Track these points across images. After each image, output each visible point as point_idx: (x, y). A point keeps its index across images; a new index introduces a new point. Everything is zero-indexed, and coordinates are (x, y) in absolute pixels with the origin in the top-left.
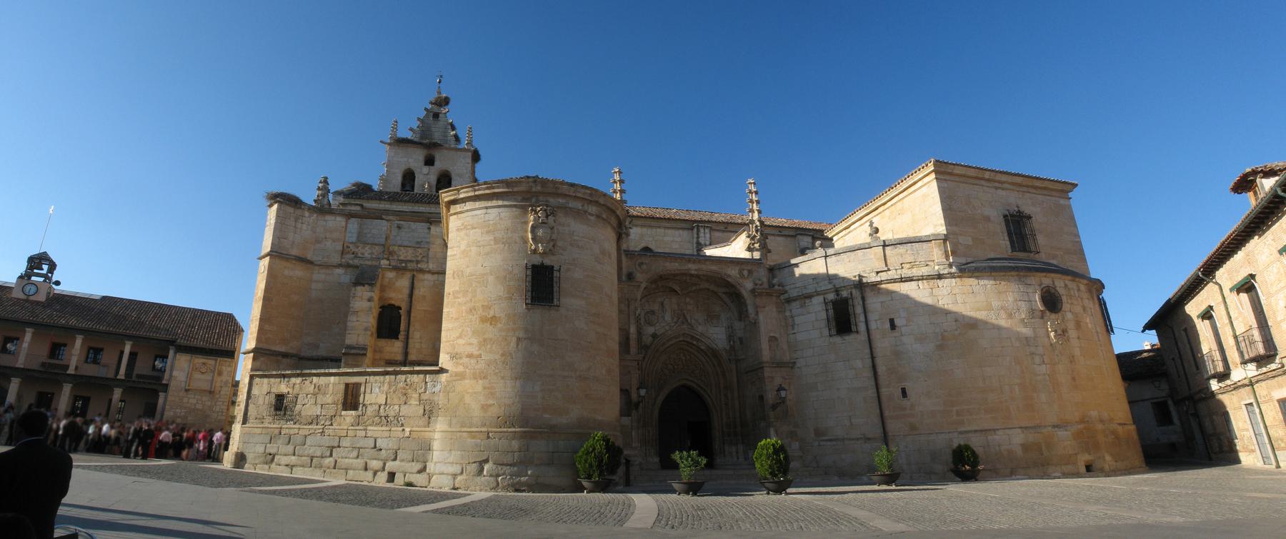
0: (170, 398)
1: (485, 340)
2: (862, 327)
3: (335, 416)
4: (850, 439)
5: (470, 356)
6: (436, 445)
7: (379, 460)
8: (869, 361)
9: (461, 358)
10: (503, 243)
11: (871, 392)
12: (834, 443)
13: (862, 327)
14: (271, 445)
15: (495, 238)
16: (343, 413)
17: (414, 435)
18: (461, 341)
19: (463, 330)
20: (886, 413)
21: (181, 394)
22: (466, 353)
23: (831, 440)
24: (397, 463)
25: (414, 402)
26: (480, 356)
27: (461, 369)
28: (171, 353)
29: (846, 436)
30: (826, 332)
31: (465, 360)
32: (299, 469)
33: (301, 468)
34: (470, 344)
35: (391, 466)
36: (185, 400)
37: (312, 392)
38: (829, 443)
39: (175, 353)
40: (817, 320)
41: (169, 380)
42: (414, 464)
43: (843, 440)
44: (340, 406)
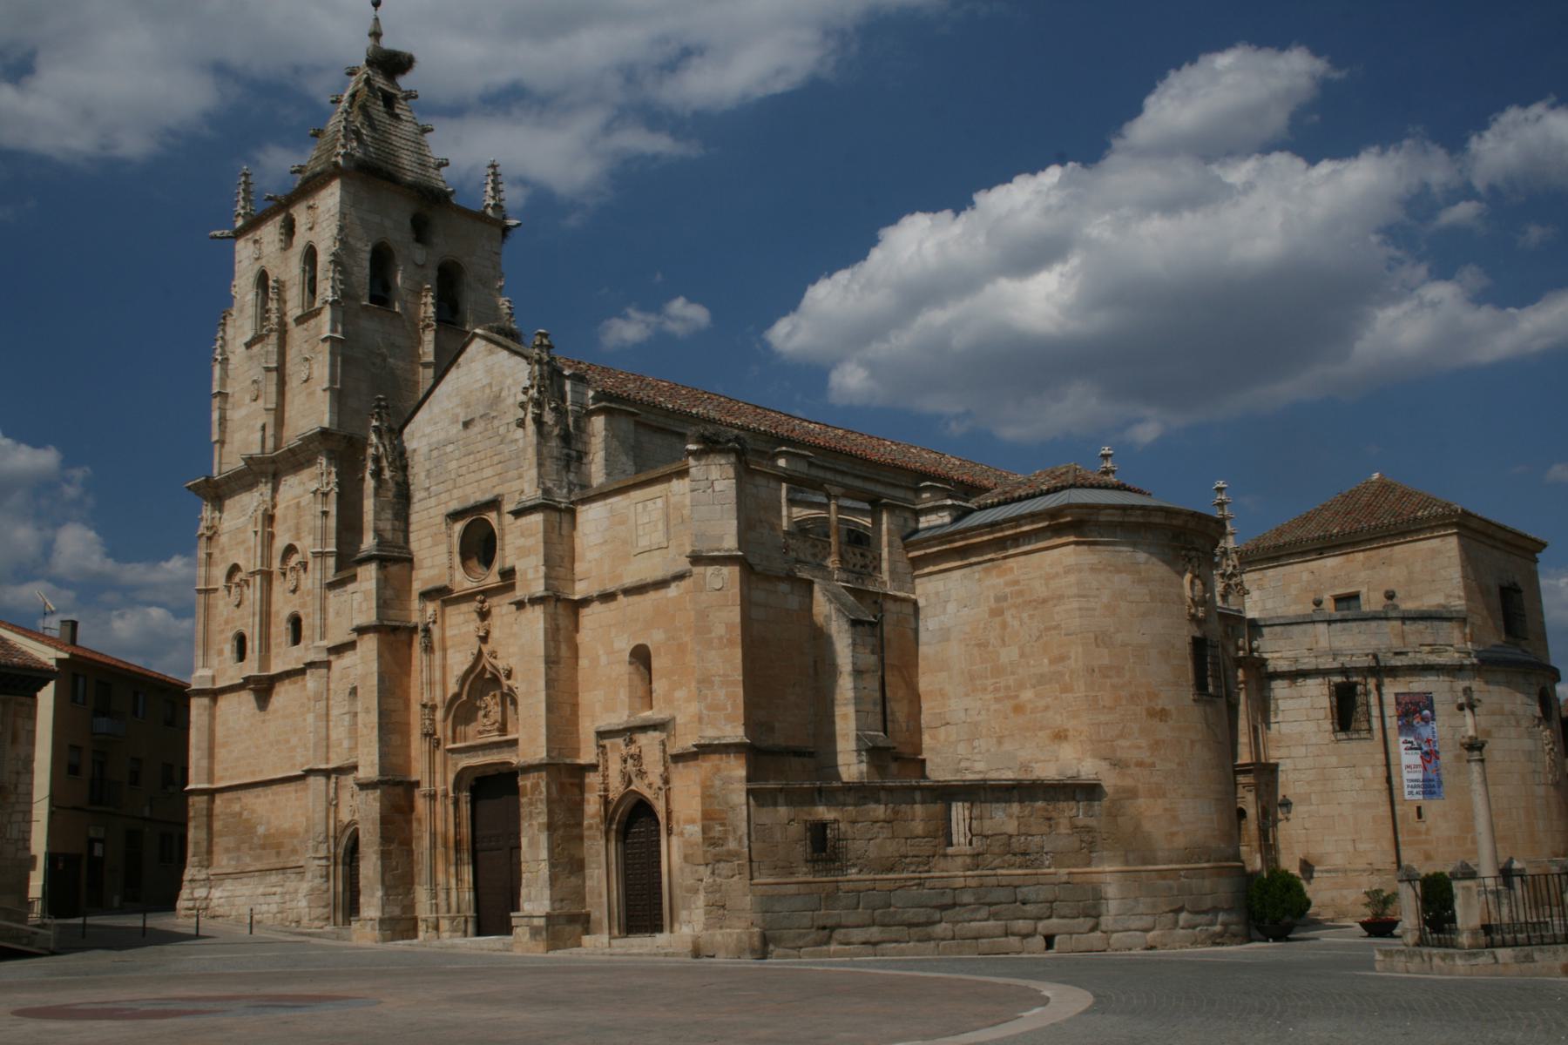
1: (1157, 743)
2: (1376, 724)
3: (934, 856)
4: (1355, 871)
5: (1140, 764)
6: (1111, 891)
7: (1025, 919)
8: (1381, 771)
9: (1128, 766)
10: (1161, 601)
11: (1384, 810)
12: (1333, 875)
13: (1376, 724)
14: (822, 912)
15: (1150, 591)
17: (1078, 879)
18: (1123, 743)
19: (1124, 727)
20: (1400, 839)
22: (1134, 760)
23: (1327, 871)
24: (1054, 921)
25: (1064, 829)
26: (1153, 765)
27: (1129, 782)
29: (1348, 866)
30: (1327, 725)
31: (1134, 770)
34: (1139, 747)
35: (1042, 926)
37: (882, 817)
38: (1325, 875)
40: (1313, 708)
42: (1081, 920)
43: (1345, 871)
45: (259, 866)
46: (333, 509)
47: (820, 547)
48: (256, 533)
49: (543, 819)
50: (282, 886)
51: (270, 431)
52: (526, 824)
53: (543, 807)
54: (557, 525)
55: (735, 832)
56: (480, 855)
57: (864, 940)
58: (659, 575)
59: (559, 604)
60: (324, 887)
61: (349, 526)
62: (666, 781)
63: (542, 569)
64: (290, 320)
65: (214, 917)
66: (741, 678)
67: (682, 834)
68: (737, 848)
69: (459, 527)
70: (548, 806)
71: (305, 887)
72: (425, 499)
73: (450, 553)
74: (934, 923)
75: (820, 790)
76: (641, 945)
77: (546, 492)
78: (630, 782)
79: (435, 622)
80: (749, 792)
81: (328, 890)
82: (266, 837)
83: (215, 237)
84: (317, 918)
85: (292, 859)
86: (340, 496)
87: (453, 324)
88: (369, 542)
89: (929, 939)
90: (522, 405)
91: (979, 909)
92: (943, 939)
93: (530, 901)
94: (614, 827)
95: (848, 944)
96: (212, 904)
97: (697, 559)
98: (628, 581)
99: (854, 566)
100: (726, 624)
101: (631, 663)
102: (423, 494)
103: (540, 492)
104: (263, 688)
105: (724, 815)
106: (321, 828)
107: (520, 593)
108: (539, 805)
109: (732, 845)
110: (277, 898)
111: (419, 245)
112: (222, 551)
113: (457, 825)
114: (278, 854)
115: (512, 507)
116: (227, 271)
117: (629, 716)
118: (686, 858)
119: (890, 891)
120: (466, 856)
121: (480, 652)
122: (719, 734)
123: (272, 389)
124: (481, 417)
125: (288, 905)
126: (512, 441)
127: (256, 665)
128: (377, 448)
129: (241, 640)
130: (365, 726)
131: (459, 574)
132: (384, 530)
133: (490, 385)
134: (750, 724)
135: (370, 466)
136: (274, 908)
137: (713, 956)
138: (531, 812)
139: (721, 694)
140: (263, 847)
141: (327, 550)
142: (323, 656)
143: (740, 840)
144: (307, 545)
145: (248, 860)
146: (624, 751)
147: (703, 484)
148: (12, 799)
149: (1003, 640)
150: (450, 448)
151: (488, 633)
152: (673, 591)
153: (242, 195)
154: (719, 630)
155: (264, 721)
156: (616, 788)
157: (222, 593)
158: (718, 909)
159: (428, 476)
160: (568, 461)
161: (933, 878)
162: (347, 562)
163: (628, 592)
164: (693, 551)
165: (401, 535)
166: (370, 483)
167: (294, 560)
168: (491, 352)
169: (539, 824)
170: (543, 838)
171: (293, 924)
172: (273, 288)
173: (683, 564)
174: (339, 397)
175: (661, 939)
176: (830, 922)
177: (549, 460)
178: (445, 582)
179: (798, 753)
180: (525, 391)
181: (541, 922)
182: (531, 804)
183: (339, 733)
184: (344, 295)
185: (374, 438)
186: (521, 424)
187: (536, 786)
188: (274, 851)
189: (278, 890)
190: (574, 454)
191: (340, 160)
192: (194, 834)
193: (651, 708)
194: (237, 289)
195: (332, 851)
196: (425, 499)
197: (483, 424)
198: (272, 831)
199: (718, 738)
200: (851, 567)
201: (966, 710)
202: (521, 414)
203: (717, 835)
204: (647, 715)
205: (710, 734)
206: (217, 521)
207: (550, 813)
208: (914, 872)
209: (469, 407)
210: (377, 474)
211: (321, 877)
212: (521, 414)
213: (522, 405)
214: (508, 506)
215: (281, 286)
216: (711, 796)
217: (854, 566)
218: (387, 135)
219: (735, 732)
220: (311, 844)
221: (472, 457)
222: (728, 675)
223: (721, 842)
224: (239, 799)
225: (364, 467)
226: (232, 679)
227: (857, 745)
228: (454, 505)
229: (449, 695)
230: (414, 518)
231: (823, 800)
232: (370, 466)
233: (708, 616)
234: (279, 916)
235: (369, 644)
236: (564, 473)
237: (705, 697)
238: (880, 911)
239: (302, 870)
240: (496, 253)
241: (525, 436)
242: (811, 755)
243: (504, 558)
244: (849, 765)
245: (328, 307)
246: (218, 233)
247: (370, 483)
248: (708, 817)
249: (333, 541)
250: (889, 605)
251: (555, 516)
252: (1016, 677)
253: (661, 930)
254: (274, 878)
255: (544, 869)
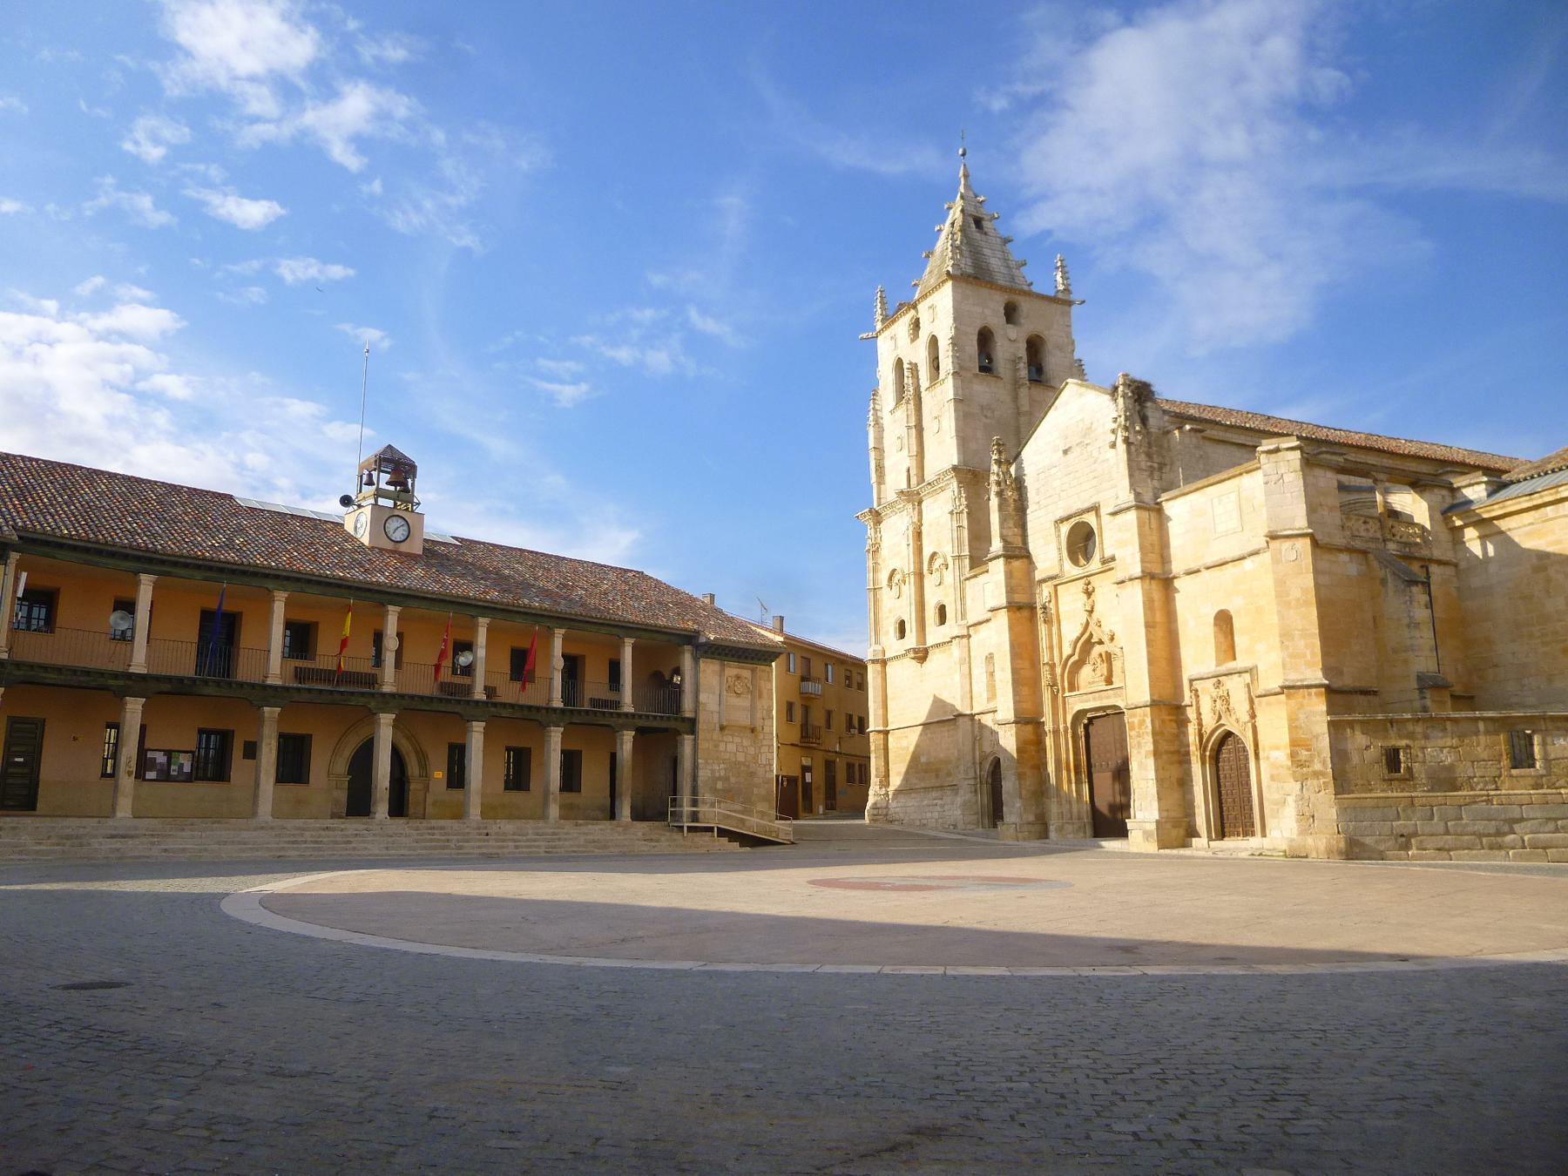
0: (702, 745)
3: (1500, 776)
16: (1514, 772)
21: (716, 735)
28: (687, 660)
32: (1462, 852)
33: (1466, 851)
36: (722, 747)
39: (696, 660)
41: (696, 711)
44: (1505, 762)
45: (923, 785)
46: (965, 524)
47: (1371, 523)
48: (908, 545)
49: (1151, 748)
50: (942, 799)
51: (913, 472)
52: (1136, 752)
53: (1149, 739)
54: (1147, 521)
55: (1319, 756)
56: (1094, 776)
57: (1439, 846)
58: (1237, 553)
59: (1152, 581)
60: (974, 800)
61: (979, 536)
62: (1253, 716)
63: (1138, 556)
64: (922, 389)
65: (891, 822)
66: (1317, 631)
67: (1268, 758)
68: (1321, 769)
69: (1065, 528)
70: (1153, 737)
71: (959, 800)
72: (1036, 510)
73: (1059, 549)
74: (1505, 834)
75: (1391, 722)
76: (1237, 846)
77: (1137, 495)
78: (1220, 718)
79: (1050, 601)
80: (1330, 723)
81: (977, 801)
82: (928, 764)
83: (862, 339)
84: (969, 823)
85: (948, 779)
86: (968, 513)
87: (1040, 381)
88: (997, 545)
89: (1500, 847)
90: (1113, 431)
91: (1547, 823)
92: (1513, 848)
93: (1141, 810)
94: (1208, 753)
95: (1425, 849)
96: (890, 813)
97: (1273, 537)
98: (1210, 561)
99: (1401, 537)
100: (1301, 588)
101: (1215, 624)
102: (1036, 507)
103: (1132, 496)
104: (922, 655)
105: (1308, 743)
106: (969, 758)
107: (1120, 575)
108: (1146, 737)
109: (1317, 766)
110: (938, 808)
111: (1009, 325)
112: (884, 561)
113: (1076, 754)
114: (937, 776)
115: (1112, 510)
116: (873, 361)
117: (1217, 666)
118: (1273, 778)
119: (1461, 806)
120: (1084, 777)
121: (1088, 623)
122: (1302, 677)
123: (914, 441)
124: (1077, 445)
125: (946, 813)
126: (1103, 461)
127: (914, 640)
128: (998, 475)
129: (902, 624)
130: (1001, 681)
131: (1067, 564)
132: (1007, 536)
133: (1083, 420)
134: (1327, 670)
135: (994, 489)
136: (936, 815)
137: (1306, 857)
138: (1139, 743)
139: (1302, 643)
140: (926, 771)
141: (962, 554)
142: (965, 632)
143: (1324, 763)
144: (948, 550)
145: (915, 781)
146: (1214, 693)
147: (1274, 478)
148: (761, 737)
149: (1548, 592)
150: (1053, 471)
151: (1092, 608)
152: (1248, 564)
153: (879, 305)
154: (1295, 593)
155: (921, 681)
156: (1209, 722)
157: (886, 589)
158: (1307, 818)
159: (1038, 494)
160: (1152, 471)
161: (1500, 795)
162: (978, 560)
163: (1208, 568)
164: (1270, 532)
165: (1020, 539)
166: (994, 502)
167: (938, 562)
168: (1081, 395)
169: (1147, 751)
170: (1151, 762)
171: (951, 827)
172: (908, 369)
173: (1260, 542)
174: (963, 440)
175: (1254, 842)
176: (1405, 832)
177: (1137, 472)
178: (1055, 571)
179: (1365, 692)
180: (1115, 420)
181: (1153, 826)
182: (1139, 736)
183: (980, 687)
184: (961, 367)
185: (995, 468)
186: (1113, 445)
187: (1142, 722)
188: (934, 774)
189: (939, 802)
190: (1156, 465)
191: (950, 269)
192: (875, 764)
193: (1235, 659)
194: (880, 373)
195: (978, 773)
196: (1036, 510)
197: (1078, 449)
198: (932, 760)
199: (1301, 680)
200: (1398, 538)
201: (1514, 653)
202: (1113, 438)
203: (1304, 758)
204: (1231, 665)
205: (1294, 677)
206: (879, 541)
207: (1155, 743)
208: (1481, 790)
209: (1067, 438)
210: (1000, 494)
211: (971, 792)
212: (1113, 438)
213: (1113, 431)
214: (1104, 511)
215: (914, 368)
216: (1296, 727)
217: (1401, 537)
218: (980, 249)
219: (1316, 676)
220: (962, 768)
221: (1071, 476)
222: (1307, 630)
223: (1307, 764)
224: (907, 737)
225: (988, 491)
226: (896, 652)
227: (1418, 684)
228: (1061, 513)
229: (1064, 657)
230: (1029, 525)
231: (1395, 729)
232: (994, 489)
233: (1285, 583)
234: (940, 821)
235: (1002, 619)
236: (1149, 481)
237: (1288, 647)
238: (1453, 823)
239: (955, 787)
240: (1067, 326)
241: (1117, 455)
242: (1375, 693)
243: (1102, 550)
244: (1411, 701)
245: (950, 377)
246: (865, 336)
247: (994, 502)
248: (1295, 743)
249: (967, 547)
250: (1434, 568)
251: (1145, 514)
252: (1563, 623)
253: (1253, 834)
254: (934, 794)
255: (1152, 788)
